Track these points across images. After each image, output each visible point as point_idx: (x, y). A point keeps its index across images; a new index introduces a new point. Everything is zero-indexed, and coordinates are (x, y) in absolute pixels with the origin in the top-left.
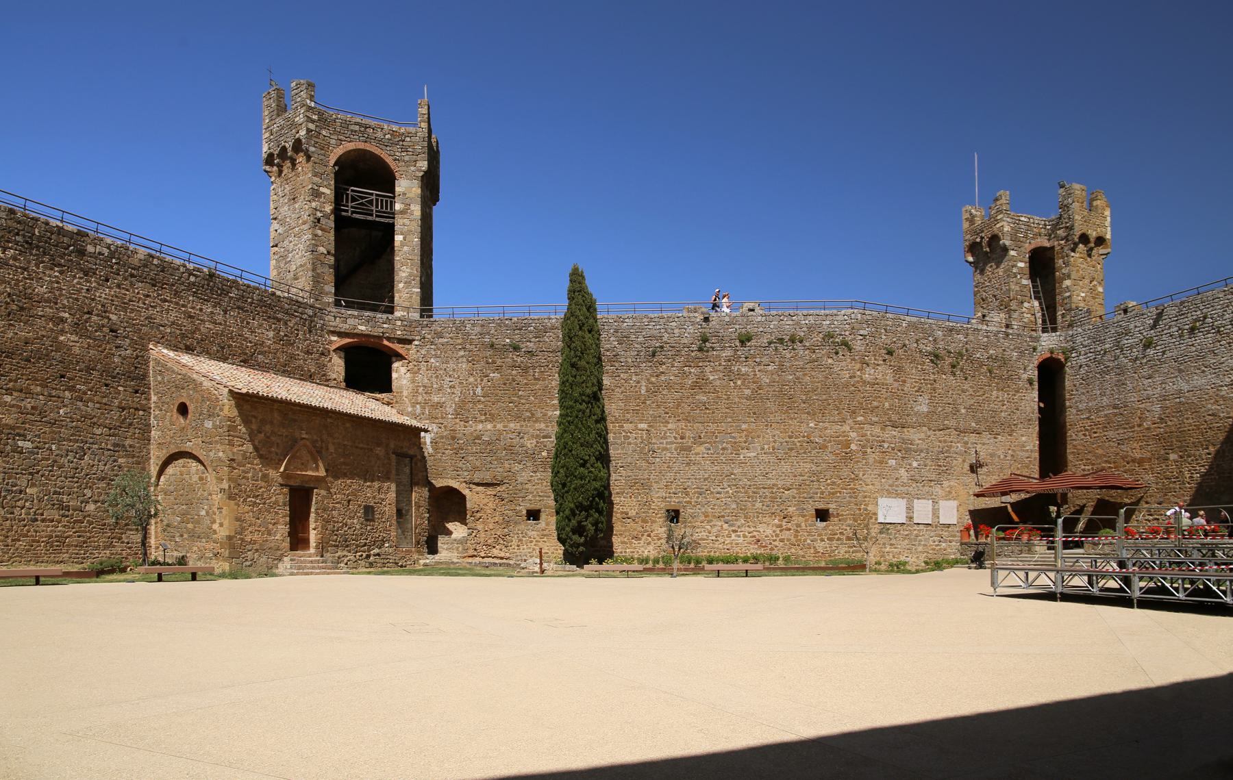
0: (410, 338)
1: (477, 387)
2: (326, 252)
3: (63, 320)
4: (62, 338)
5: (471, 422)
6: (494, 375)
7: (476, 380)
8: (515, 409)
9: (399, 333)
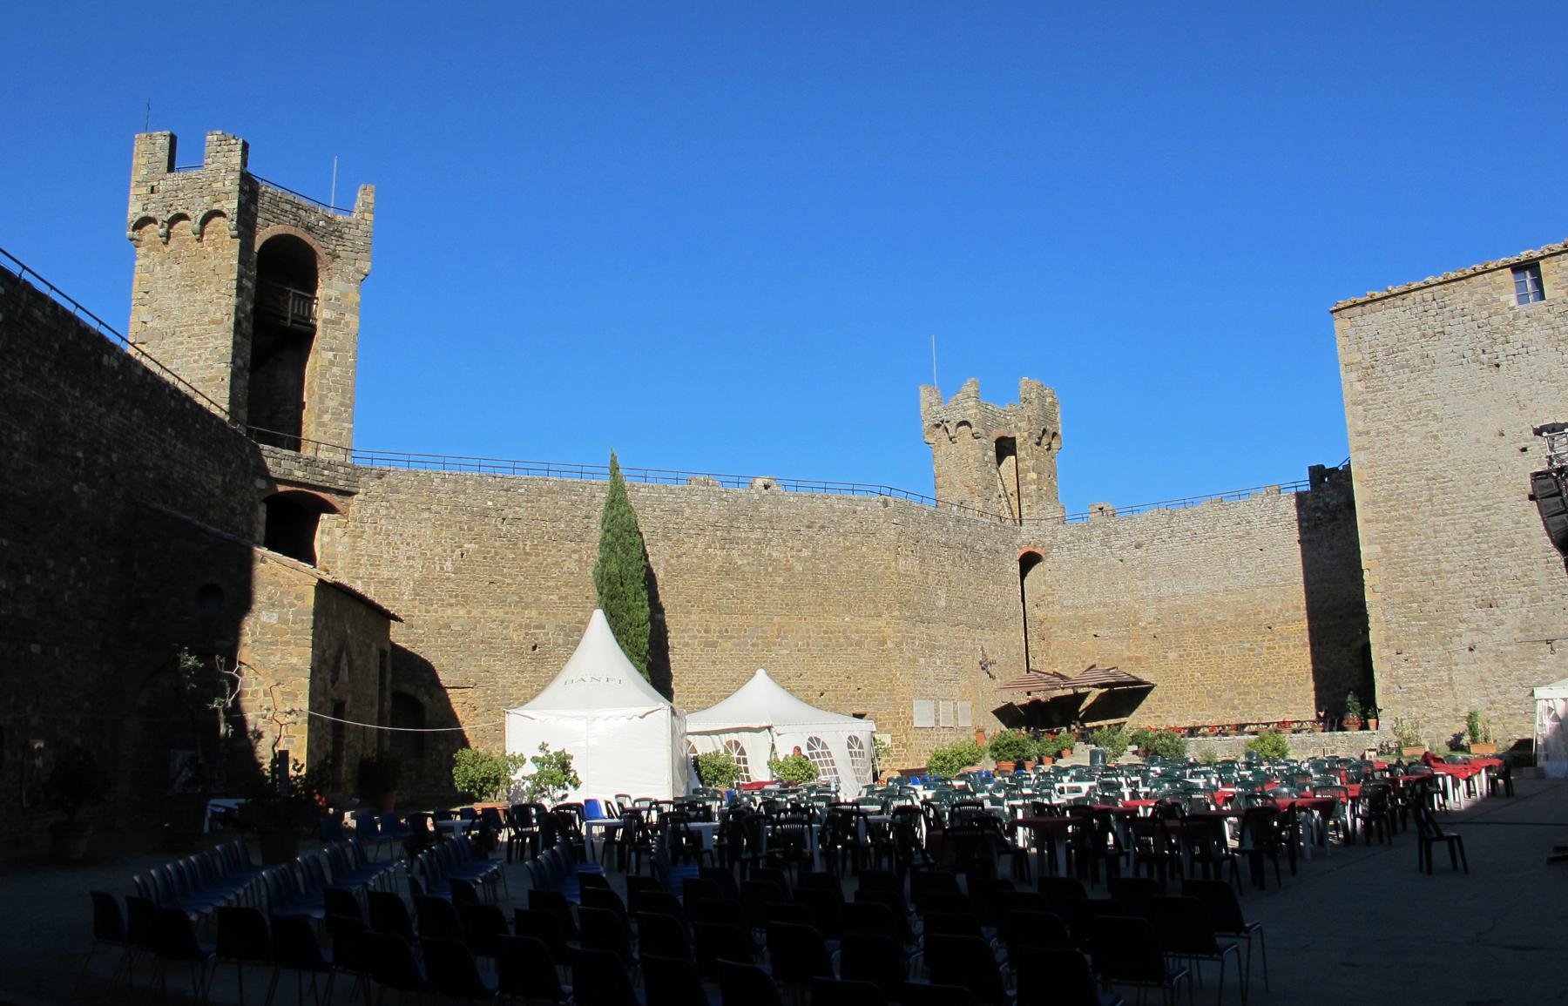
0: (354, 490)
1: (446, 561)
5: (435, 606)
6: (470, 546)
7: (445, 551)
8: (498, 591)
9: (341, 483)
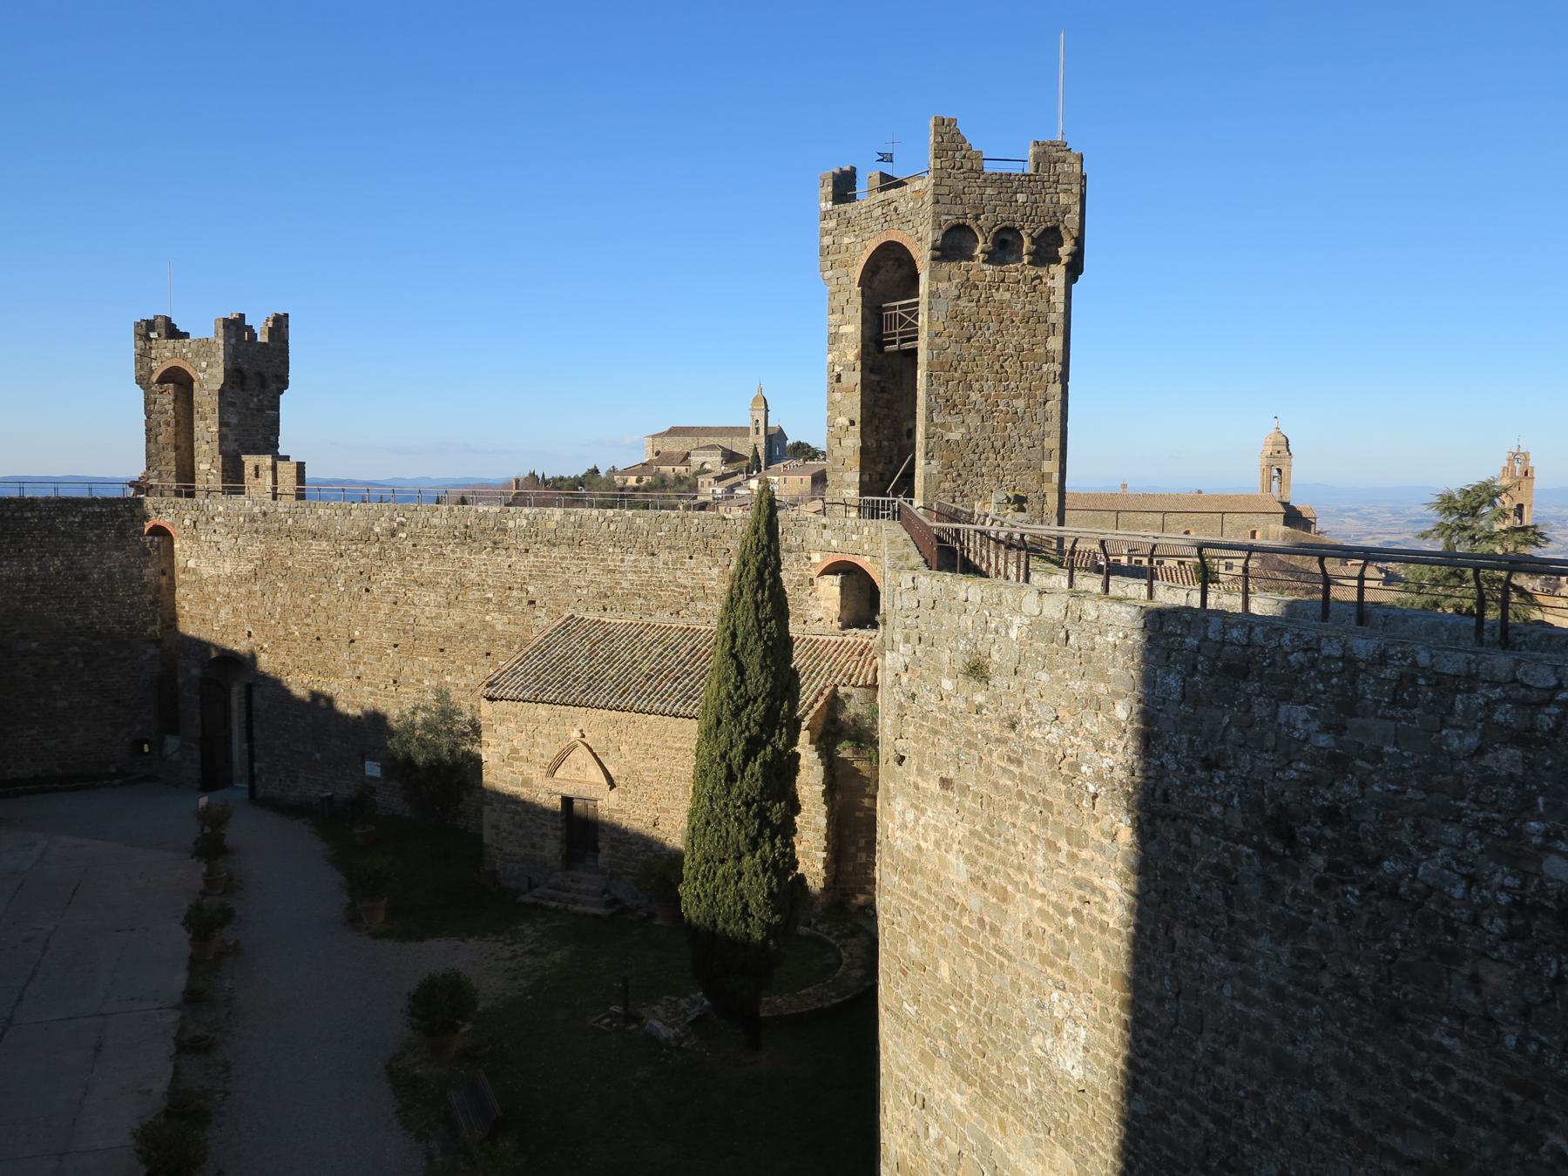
2: (847, 423)
3: (489, 600)
4: (488, 618)
